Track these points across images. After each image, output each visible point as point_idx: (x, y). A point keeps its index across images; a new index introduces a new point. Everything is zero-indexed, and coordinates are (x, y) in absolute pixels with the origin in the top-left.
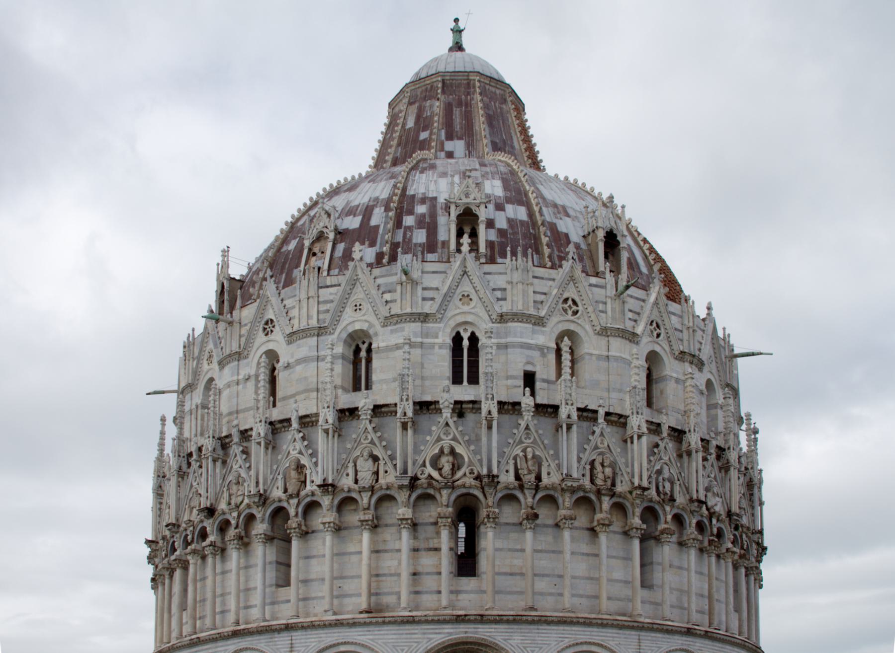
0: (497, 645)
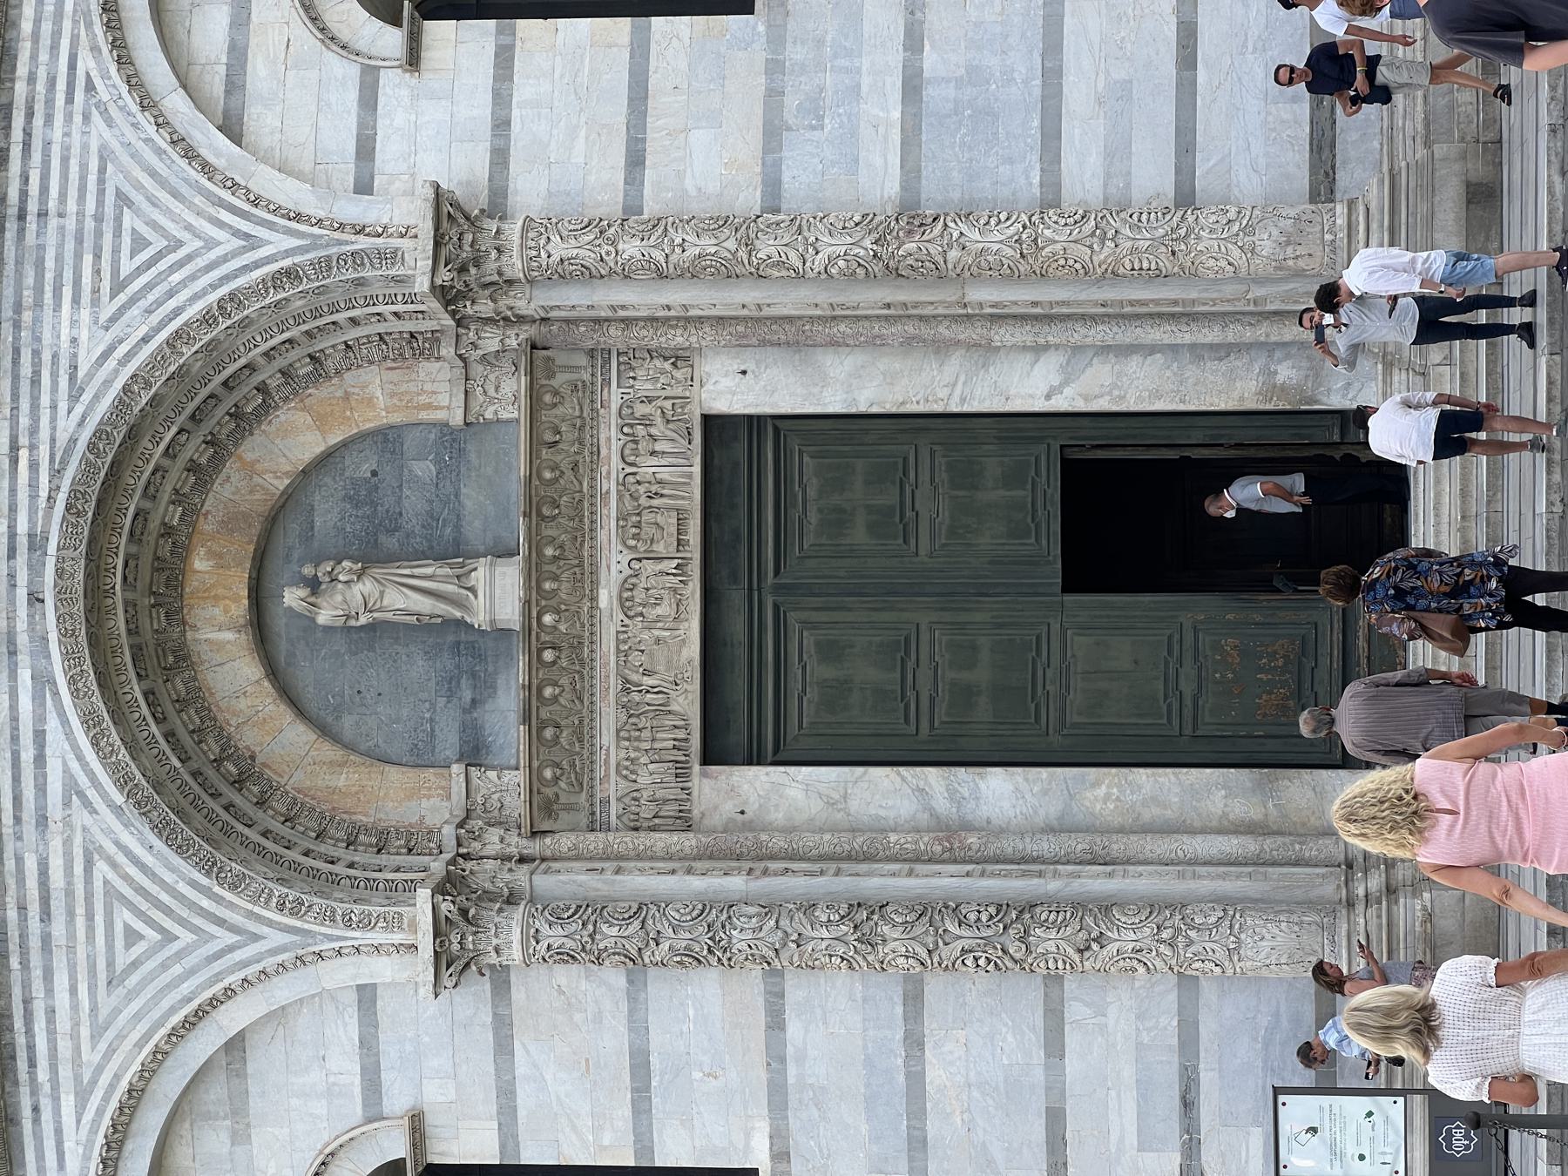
0: (98, 434)
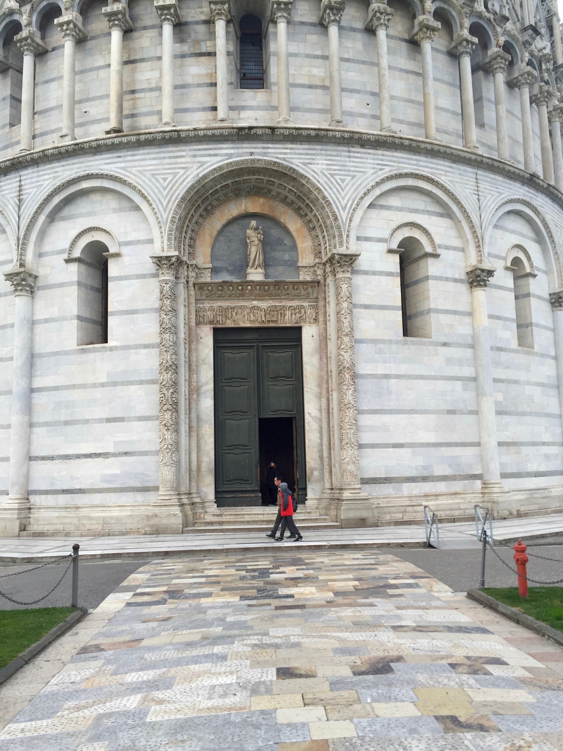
0: (294, 170)
